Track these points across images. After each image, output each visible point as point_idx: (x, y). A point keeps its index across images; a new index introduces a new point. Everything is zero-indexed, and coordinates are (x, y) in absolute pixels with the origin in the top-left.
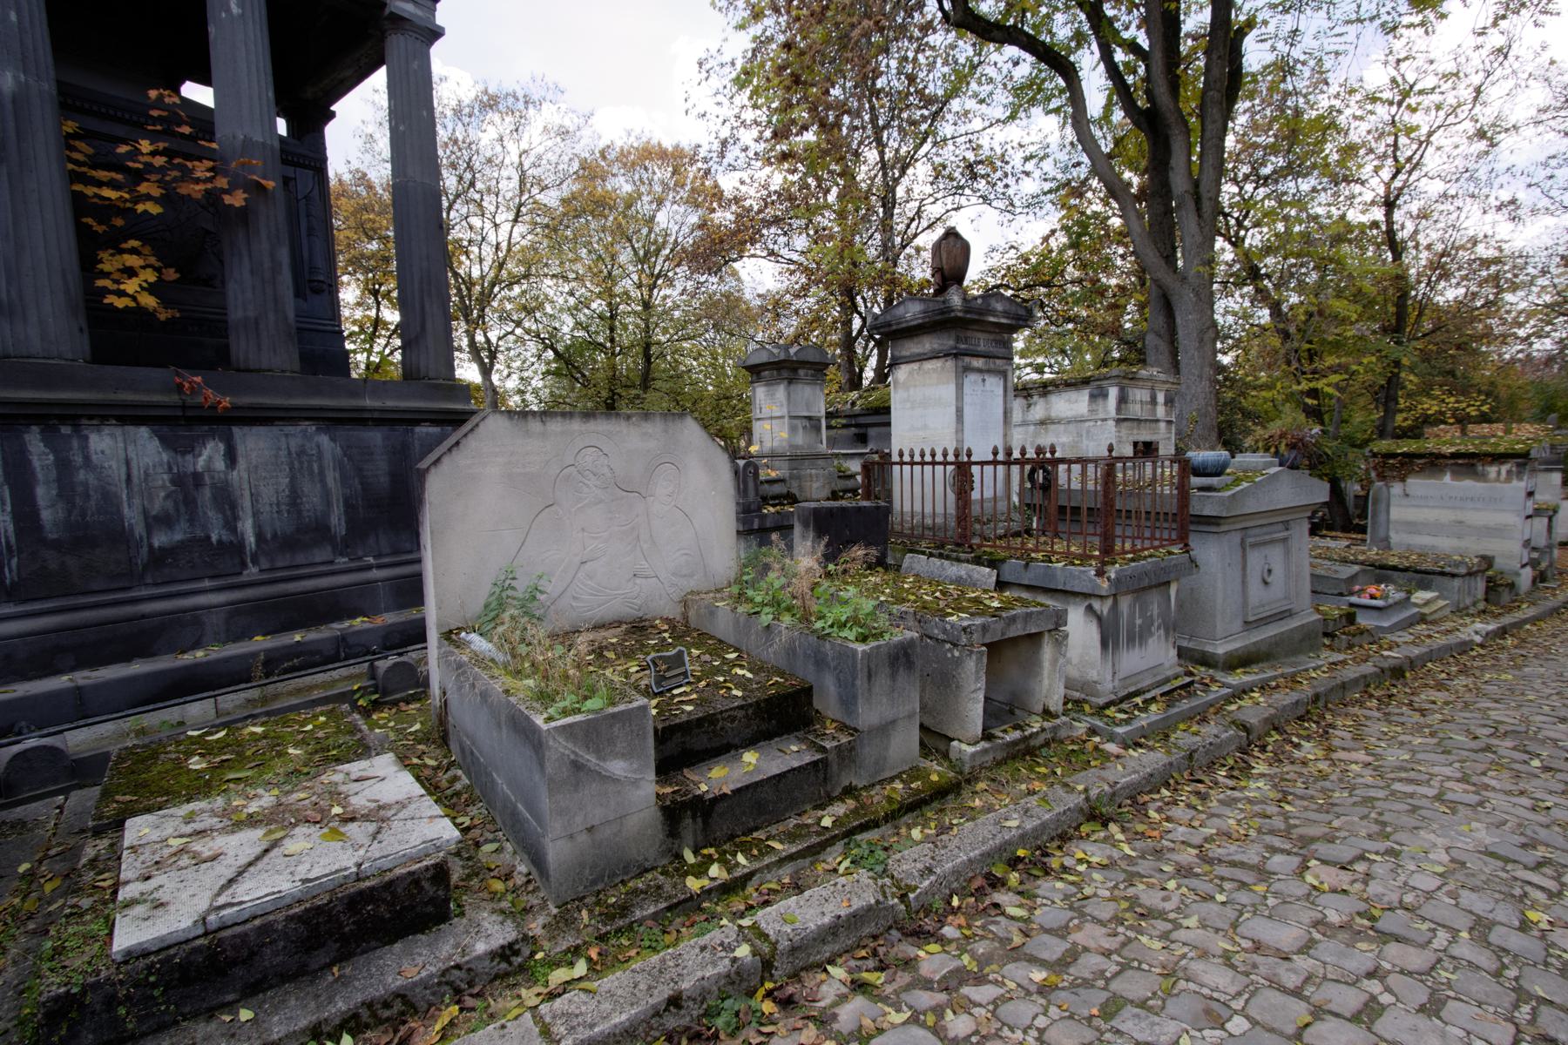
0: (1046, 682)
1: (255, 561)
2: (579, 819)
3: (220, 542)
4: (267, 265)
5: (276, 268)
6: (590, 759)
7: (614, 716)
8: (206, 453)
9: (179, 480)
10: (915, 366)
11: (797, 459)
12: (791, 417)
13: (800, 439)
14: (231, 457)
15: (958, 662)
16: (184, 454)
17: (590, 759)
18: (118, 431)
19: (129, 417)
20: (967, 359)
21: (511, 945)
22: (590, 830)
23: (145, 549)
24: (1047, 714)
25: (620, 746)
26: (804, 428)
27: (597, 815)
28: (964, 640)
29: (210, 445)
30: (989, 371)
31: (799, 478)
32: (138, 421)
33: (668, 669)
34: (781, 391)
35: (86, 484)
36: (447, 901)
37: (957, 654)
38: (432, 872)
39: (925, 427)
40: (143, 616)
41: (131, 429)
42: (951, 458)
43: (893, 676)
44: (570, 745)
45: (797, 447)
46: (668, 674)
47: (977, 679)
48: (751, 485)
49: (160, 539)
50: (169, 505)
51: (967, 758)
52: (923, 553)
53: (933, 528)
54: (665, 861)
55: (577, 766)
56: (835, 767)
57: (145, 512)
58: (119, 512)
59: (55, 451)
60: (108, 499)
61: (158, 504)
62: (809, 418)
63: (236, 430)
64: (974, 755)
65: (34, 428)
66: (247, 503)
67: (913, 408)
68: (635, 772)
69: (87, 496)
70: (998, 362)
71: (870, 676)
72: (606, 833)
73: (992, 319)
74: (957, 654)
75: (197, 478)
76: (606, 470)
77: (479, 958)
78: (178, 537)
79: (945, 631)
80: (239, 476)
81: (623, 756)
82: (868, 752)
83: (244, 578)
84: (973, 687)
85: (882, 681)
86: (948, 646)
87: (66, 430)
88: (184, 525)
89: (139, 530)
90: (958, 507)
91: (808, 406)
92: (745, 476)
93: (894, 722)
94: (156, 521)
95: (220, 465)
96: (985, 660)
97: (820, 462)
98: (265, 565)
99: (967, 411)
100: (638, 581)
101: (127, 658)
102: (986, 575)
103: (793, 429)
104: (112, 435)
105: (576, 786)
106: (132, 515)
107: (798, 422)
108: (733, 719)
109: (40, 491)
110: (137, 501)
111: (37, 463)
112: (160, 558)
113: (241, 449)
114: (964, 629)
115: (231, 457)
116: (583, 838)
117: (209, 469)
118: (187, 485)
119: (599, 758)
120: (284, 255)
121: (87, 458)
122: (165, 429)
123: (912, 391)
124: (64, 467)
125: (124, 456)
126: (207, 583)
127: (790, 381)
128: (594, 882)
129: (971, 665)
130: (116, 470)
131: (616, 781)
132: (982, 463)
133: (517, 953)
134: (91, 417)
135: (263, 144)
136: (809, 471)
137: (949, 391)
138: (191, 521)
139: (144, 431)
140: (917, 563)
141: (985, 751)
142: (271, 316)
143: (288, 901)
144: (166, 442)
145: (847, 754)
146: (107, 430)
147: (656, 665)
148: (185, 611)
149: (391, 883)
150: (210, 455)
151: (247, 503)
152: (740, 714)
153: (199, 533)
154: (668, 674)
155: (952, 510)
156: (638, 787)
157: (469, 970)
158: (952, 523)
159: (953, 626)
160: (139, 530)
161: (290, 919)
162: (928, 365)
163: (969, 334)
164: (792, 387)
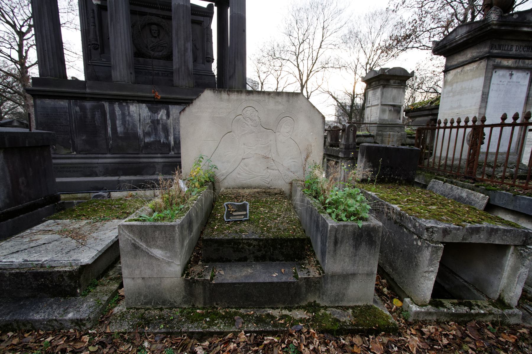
0: (504, 281)
1: (173, 151)
2: (137, 272)
3: (163, 142)
4: (183, 49)
5: (186, 50)
6: (143, 245)
7: (155, 226)
8: (161, 113)
9: (153, 122)
10: (459, 70)
11: (382, 126)
12: (382, 105)
13: (387, 116)
14: (168, 115)
15: (419, 249)
16: (155, 113)
17: (143, 245)
18: (137, 105)
19: (140, 100)
20: (498, 60)
21: (81, 320)
22: (143, 278)
23: (143, 143)
24: (501, 303)
25: (159, 243)
26: (390, 111)
27: (147, 273)
28: (425, 236)
29: (162, 111)
30: (518, 68)
31: (382, 135)
32: (143, 102)
33: (235, 211)
34: (379, 92)
35: (129, 121)
36: (76, 288)
37: (420, 244)
38: (68, 274)
39: (460, 106)
40: (140, 163)
41: (141, 104)
42: (470, 123)
43: (356, 247)
44: (131, 235)
45: (384, 120)
46: (234, 214)
47: (431, 263)
48: (351, 136)
49: (147, 140)
50: (150, 129)
51: (412, 314)
52: (442, 180)
53: (452, 166)
54: (186, 306)
55: (135, 247)
56: (303, 290)
57: (143, 131)
58: (137, 130)
59: (121, 110)
60: (134, 126)
61: (147, 129)
62: (394, 106)
63: (170, 106)
64: (417, 313)
65: (117, 103)
66: (172, 131)
67: (453, 96)
68: (168, 257)
69: (129, 124)
70: (527, 61)
71: (336, 243)
72: (153, 282)
73: (525, 29)
74: (420, 244)
75: (158, 121)
76: (257, 118)
77: (65, 320)
78: (152, 140)
79: (415, 226)
80: (170, 121)
81: (161, 248)
82: (332, 288)
83: (169, 155)
84: (426, 269)
85: (346, 248)
86: (415, 237)
87: (124, 104)
88: (153, 136)
89: (142, 136)
90: (469, 154)
91: (394, 99)
92: (348, 131)
93: (354, 275)
94: (147, 134)
95: (165, 117)
96: (440, 253)
97: (396, 129)
98: (176, 152)
99: (492, 95)
100: (269, 171)
101: (135, 175)
102: (480, 199)
103: (383, 111)
104: (136, 106)
105: (135, 256)
106: (140, 132)
107: (387, 108)
108: (250, 245)
109: (117, 122)
110: (141, 127)
111: (117, 114)
112: (147, 146)
113: (171, 113)
114: (427, 229)
115: (168, 115)
116: (140, 281)
117: (161, 119)
118: (155, 123)
119: (147, 246)
120: (189, 46)
121: (129, 113)
122: (150, 105)
123: (454, 86)
124: (123, 114)
125: (139, 112)
126: (159, 155)
127: (384, 86)
128: (146, 304)
129: (427, 254)
130: (136, 116)
131: (157, 259)
132: (492, 126)
133: (84, 325)
134: (130, 100)
135: (183, 5)
136: (388, 132)
137: (479, 82)
138: (156, 135)
139: (144, 105)
140: (439, 186)
141: (430, 313)
142: (183, 67)
143: (14, 267)
144: (150, 109)
145: (314, 285)
146: (134, 105)
147: (228, 207)
148: (151, 163)
149: (51, 273)
150: (162, 114)
151: (172, 131)
152: (255, 243)
153: (158, 139)
154: (234, 214)
155: (465, 155)
156: (170, 266)
157: (61, 324)
158: (464, 163)
159: (420, 224)
160: (142, 136)
161: (11, 274)
162: (467, 68)
163: (503, 43)
164: (385, 89)
